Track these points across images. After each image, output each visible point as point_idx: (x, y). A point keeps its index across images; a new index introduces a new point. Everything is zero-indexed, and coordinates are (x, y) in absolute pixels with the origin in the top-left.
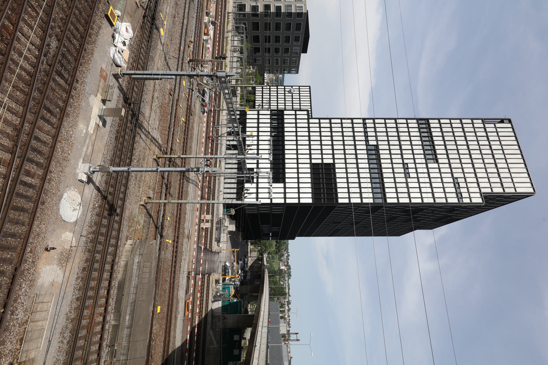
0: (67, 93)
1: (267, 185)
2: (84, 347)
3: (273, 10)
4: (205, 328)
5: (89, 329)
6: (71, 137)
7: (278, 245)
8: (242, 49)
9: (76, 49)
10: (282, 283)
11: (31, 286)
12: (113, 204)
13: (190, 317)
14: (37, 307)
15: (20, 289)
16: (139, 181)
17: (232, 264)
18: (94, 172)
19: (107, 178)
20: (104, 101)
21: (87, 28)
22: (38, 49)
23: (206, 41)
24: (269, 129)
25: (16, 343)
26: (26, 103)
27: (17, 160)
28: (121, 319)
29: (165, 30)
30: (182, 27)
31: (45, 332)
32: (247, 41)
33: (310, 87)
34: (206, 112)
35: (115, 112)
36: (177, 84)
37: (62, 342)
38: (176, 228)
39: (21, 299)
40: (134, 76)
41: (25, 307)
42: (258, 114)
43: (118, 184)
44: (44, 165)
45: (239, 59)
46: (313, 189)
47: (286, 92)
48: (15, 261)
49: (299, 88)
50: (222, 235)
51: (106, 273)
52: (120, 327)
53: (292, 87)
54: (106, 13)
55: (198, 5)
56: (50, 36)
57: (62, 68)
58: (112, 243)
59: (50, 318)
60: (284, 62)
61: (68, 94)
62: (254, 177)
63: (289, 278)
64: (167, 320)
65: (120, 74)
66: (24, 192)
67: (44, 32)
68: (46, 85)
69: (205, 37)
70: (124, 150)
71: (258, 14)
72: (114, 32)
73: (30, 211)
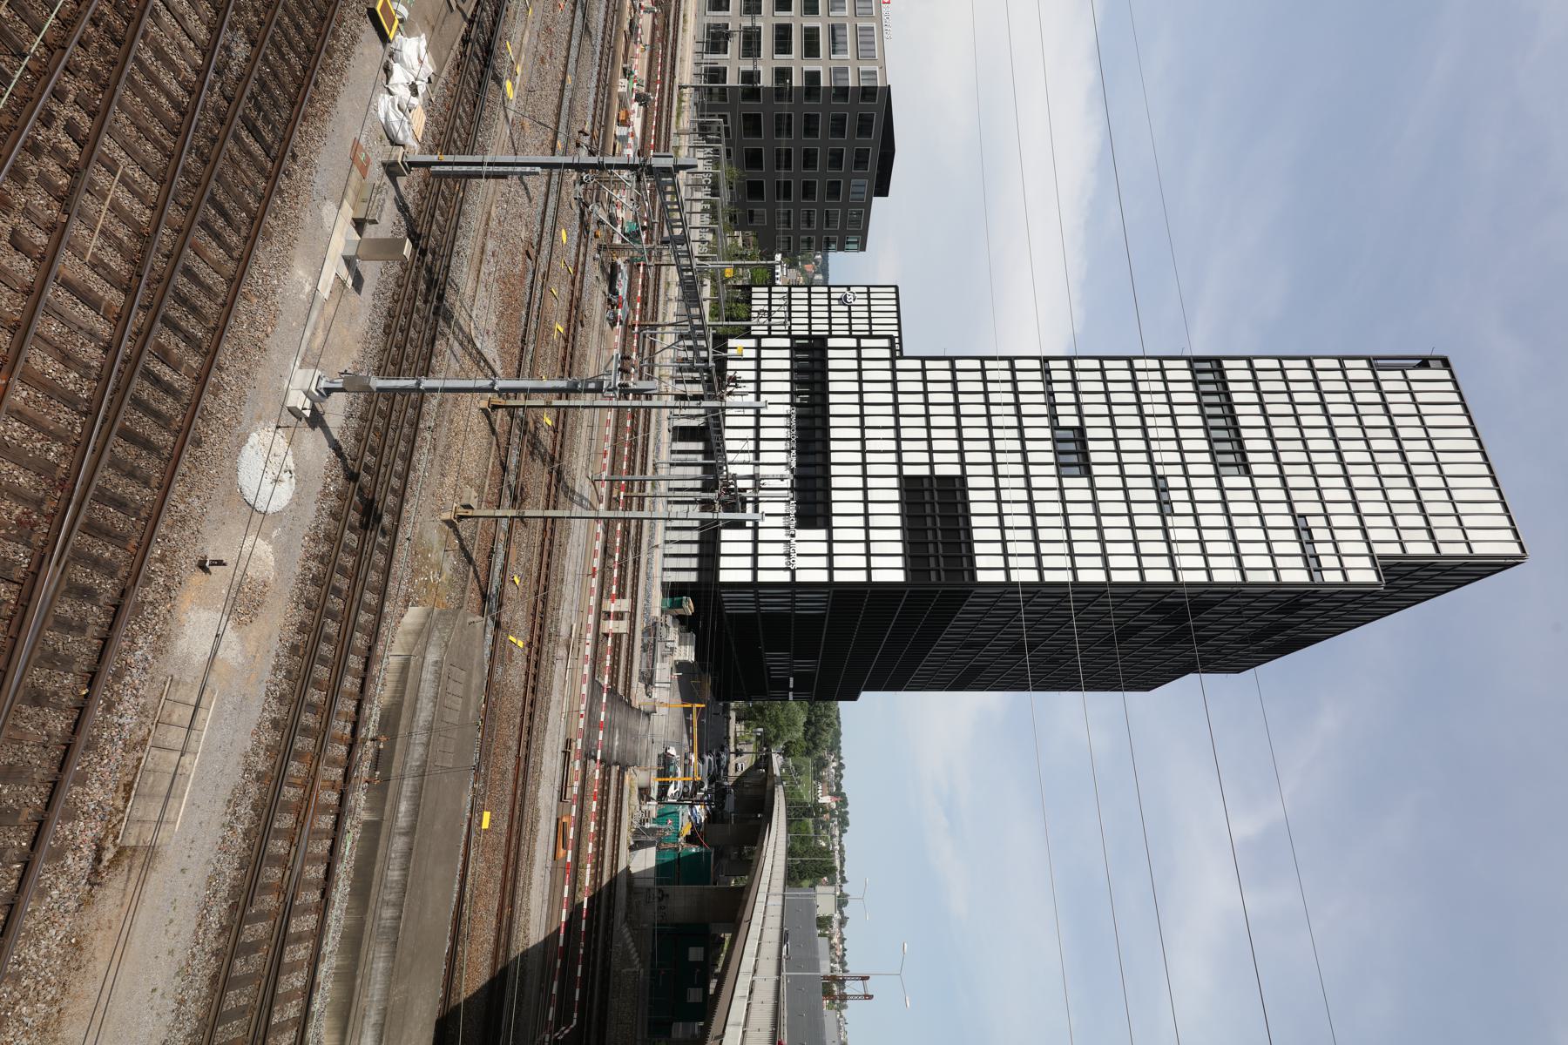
0: (267, 178)
1: (781, 535)
2: (288, 861)
3: (797, 81)
4: (610, 915)
5: (302, 813)
6: (274, 292)
7: (813, 730)
8: (715, 177)
9: (295, 78)
10: (824, 844)
11: (158, 651)
12: (373, 499)
13: (569, 860)
14: (173, 711)
15: (131, 650)
16: (442, 457)
17: (686, 758)
18: (329, 391)
19: (360, 426)
20: (359, 224)
21: (323, 31)
22: (202, 50)
23: (623, 139)
24: (787, 387)
25: (116, 792)
26: (168, 176)
27: (138, 314)
28: (388, 808)
29: (517, 86)
30: (562, 91)
31: (189, 785)
32: (730, 163)
33: (896, 287)
34: (621, 323)
35: (387, 249)
36: (545, 234)
37: (232, 828)
38: (535, 609)
39: (131, 676)
40: (438, 168)
41: (142, 701)
42: (759, 348)
43: (378, 486)
44: (205, 345)
45: (709, 206)
46: (910, 573)
47: (833, 302)
48: (122, 573)
49: (869, 290)
50: (658, 665)
51: (350, 678)
52: (384, 831)
53: (849, 289)
54: (371, 6)
55: (603, 46)
56: (232, 27)
57: (259, 115)
58: (368, 601)
59: (202, 752)
60: (828, 225)
61: (270, 181)
62: (749, 499)
63: (843, 831)
64: (507, 857)
65: (402, 162)
66: (152, 401)
67: (217, 14)
68: (217, 145)
69: (620, 131)
70: (393, 418)
71: (759, 89)
72: (388, 58)
73: (166, 453)
